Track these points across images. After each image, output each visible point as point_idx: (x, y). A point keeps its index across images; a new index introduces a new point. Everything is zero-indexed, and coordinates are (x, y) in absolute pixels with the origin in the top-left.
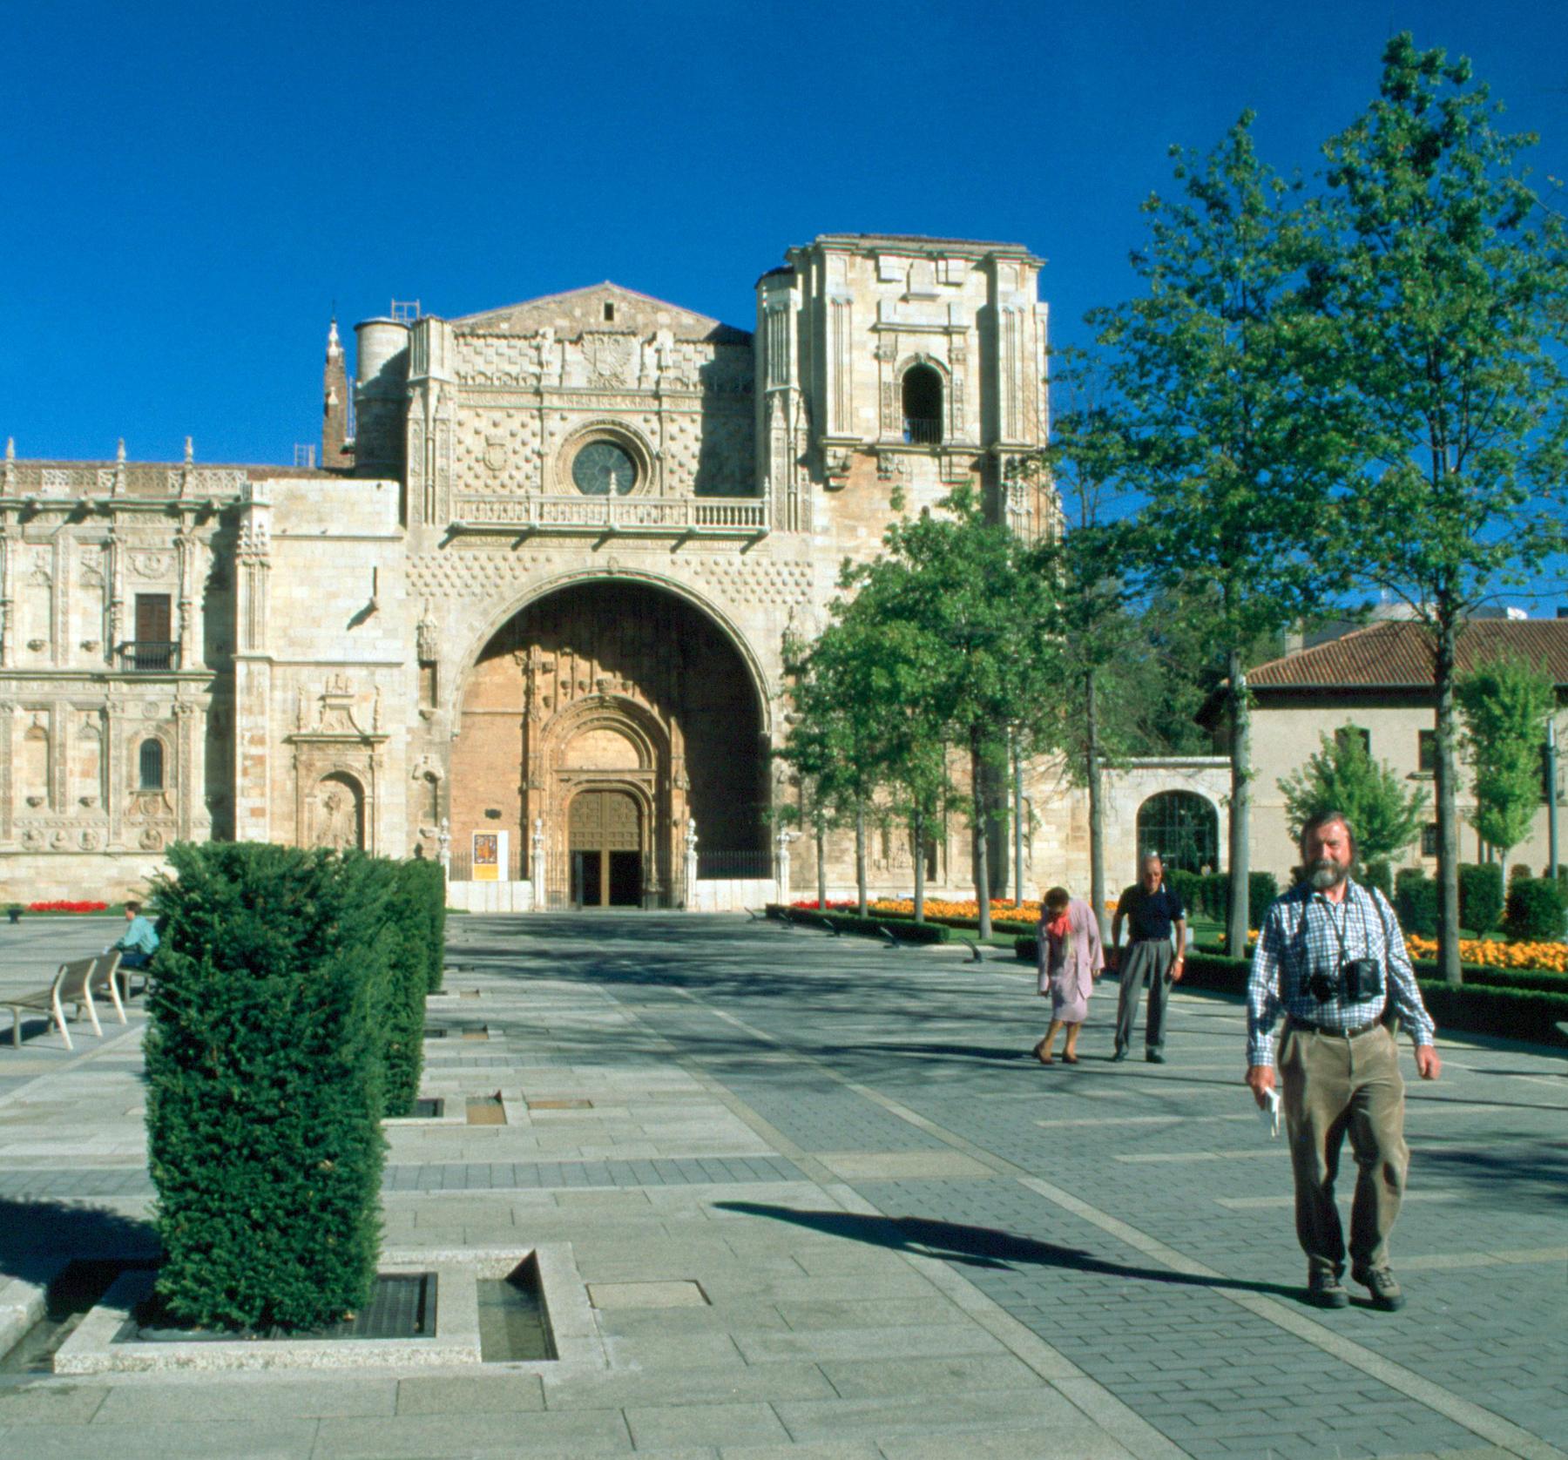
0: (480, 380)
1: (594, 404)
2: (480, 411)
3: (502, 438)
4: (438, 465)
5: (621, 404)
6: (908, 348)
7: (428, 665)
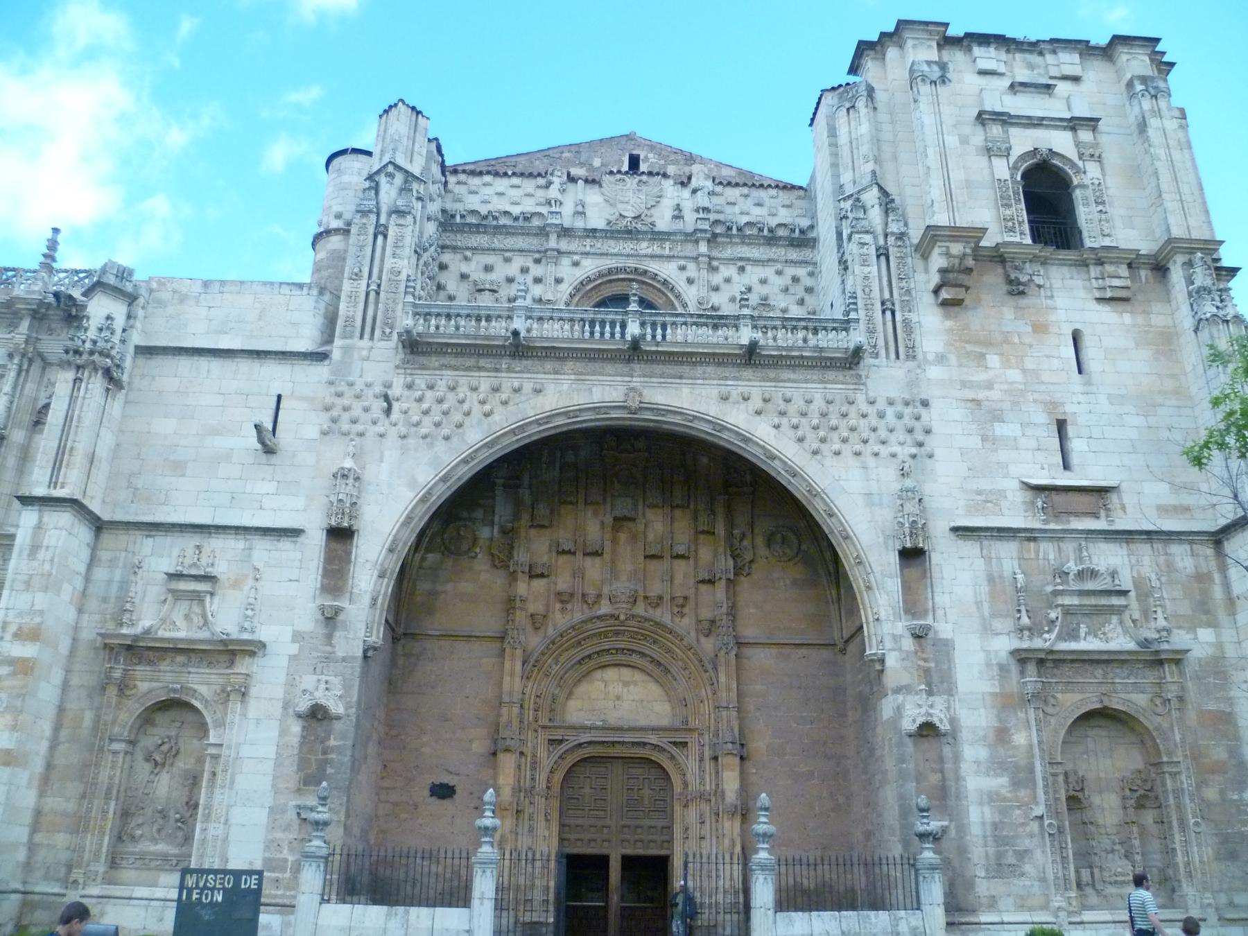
0: (472, 220)
1: (614, 246)
2: (468, 253)
3: (492, 282)
4: (387, 266)
5: (644, 247)
6: (1023, 142)
7: (340, 535)
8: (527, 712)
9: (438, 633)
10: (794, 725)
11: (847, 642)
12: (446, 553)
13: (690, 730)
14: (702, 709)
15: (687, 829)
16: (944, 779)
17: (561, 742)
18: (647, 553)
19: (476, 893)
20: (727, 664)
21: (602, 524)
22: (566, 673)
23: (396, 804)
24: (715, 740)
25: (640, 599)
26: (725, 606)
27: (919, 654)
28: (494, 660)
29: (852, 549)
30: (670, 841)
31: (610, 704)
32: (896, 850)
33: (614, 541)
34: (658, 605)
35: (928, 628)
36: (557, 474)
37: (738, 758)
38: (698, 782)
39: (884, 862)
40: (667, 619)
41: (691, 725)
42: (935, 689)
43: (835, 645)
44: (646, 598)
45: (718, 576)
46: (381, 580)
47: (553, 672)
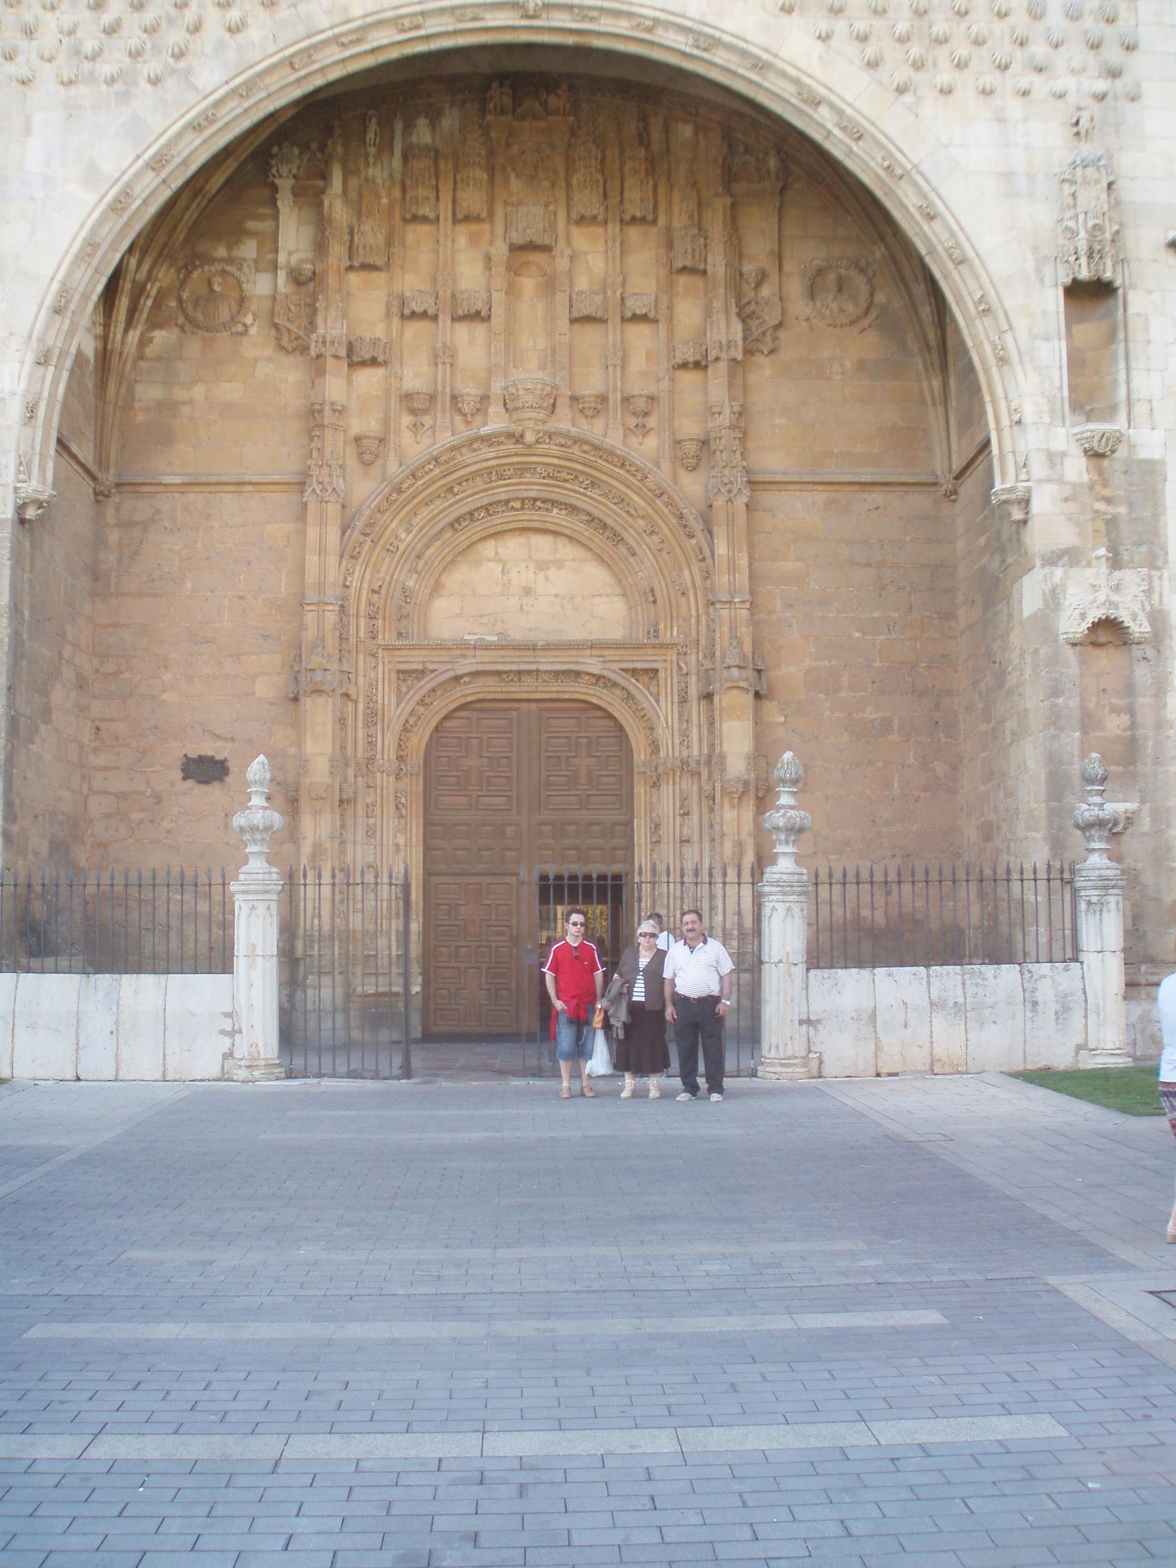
8: (353, 620)
9: (178, 480)
10: (857, 635)
11: (957, 478)
12: (188, 327)
13: (661, 646)
14: (684, 611)
15: (657, 826)
16: (1133, 726)
17: (421, 673)
18: (576, 314)
19: (240, 948)
20: (731, 522)
21: (488, 259)
22: (427, 546)
23: (121, 796)
24: (708, 664)
25: (563, 402)
26: (727, 411)
27: (1098, 488)
28: (290, 527)
29: (972, 285)
30: (630, 848)
31: (513, 602)
32: (1038, 854)
33: (512, 290)
34: (597, 412)
35: (1117, 439)
36: (397, 162)
37: (751, 696)
38: (677, 742)
39: (1015, 876)
40: (614, 440)
41: (666, 637)
42: (1126, 557)
43: (935, 484)
44: (574, 399)
45: (712, 355)
46: (41, 369)
47: (402, 547)
